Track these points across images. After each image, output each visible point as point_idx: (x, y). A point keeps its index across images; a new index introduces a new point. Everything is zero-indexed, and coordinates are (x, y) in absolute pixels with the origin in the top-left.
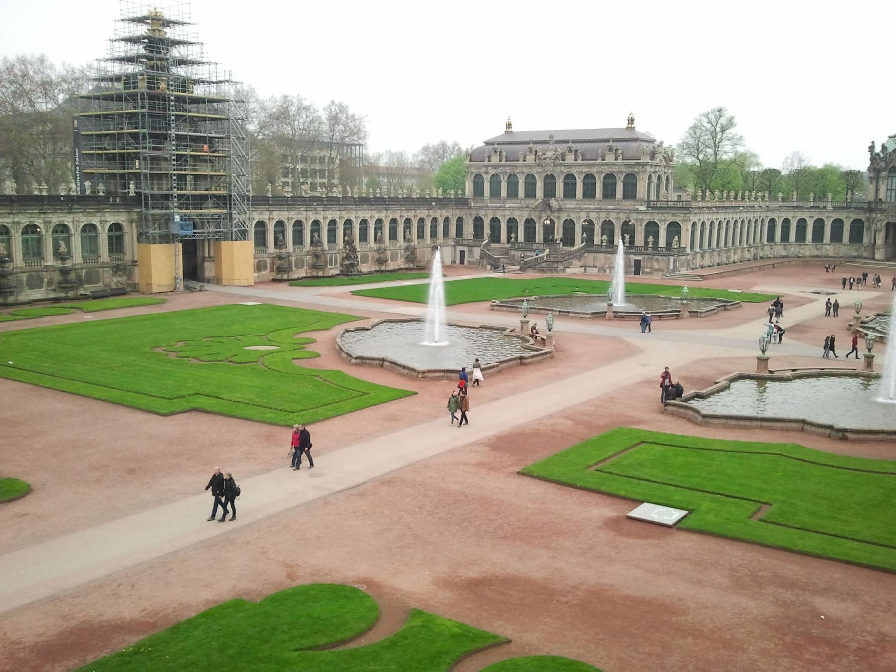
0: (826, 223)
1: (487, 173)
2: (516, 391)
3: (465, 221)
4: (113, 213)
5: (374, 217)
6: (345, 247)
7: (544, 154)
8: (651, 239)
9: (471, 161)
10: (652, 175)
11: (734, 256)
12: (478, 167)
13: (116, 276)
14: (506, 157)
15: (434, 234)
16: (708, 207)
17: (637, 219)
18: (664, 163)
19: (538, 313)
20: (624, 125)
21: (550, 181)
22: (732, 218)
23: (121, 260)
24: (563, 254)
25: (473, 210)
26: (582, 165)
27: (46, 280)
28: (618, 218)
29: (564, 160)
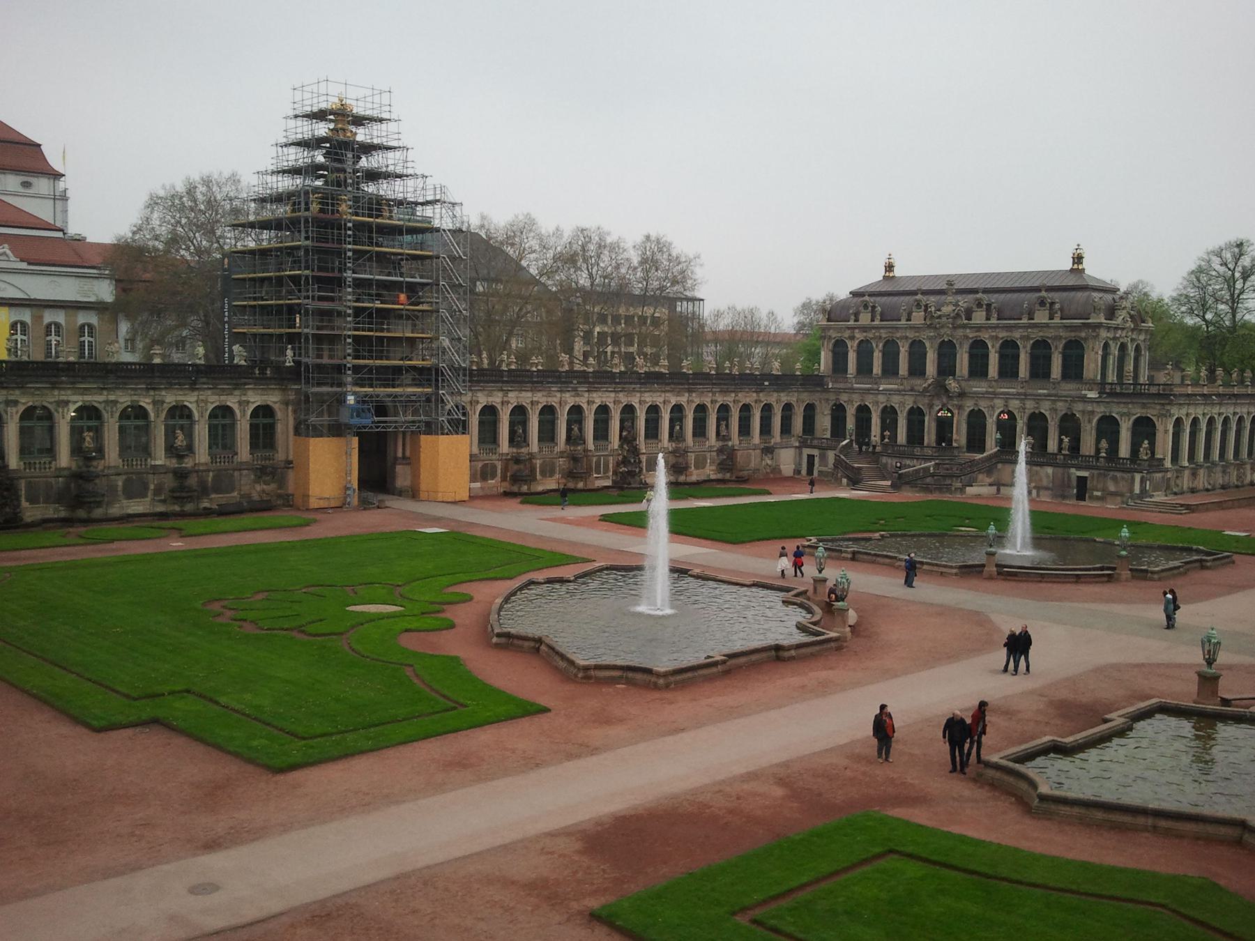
1: (852, 338)
2: (733, 712)
3: (818, 410)
4: (260, 391)
5: (670, 402)
6: (621, 446)
7: (939, 310)
9: (829, 320)
10: (1111, 342)
12: (840, 330)
13: (259, 482)
14: (882, 314)
15: (766, 429)
16: (1204, 395)
17: (1083, 412)
18: (1130, 324)
19: (873, 562)
20: (1068, 265)
21: (947, 352)
23: (270, 460)
24: (961, 465)
25: (831, 394)
27: (152, 487)
29: (970, 319)
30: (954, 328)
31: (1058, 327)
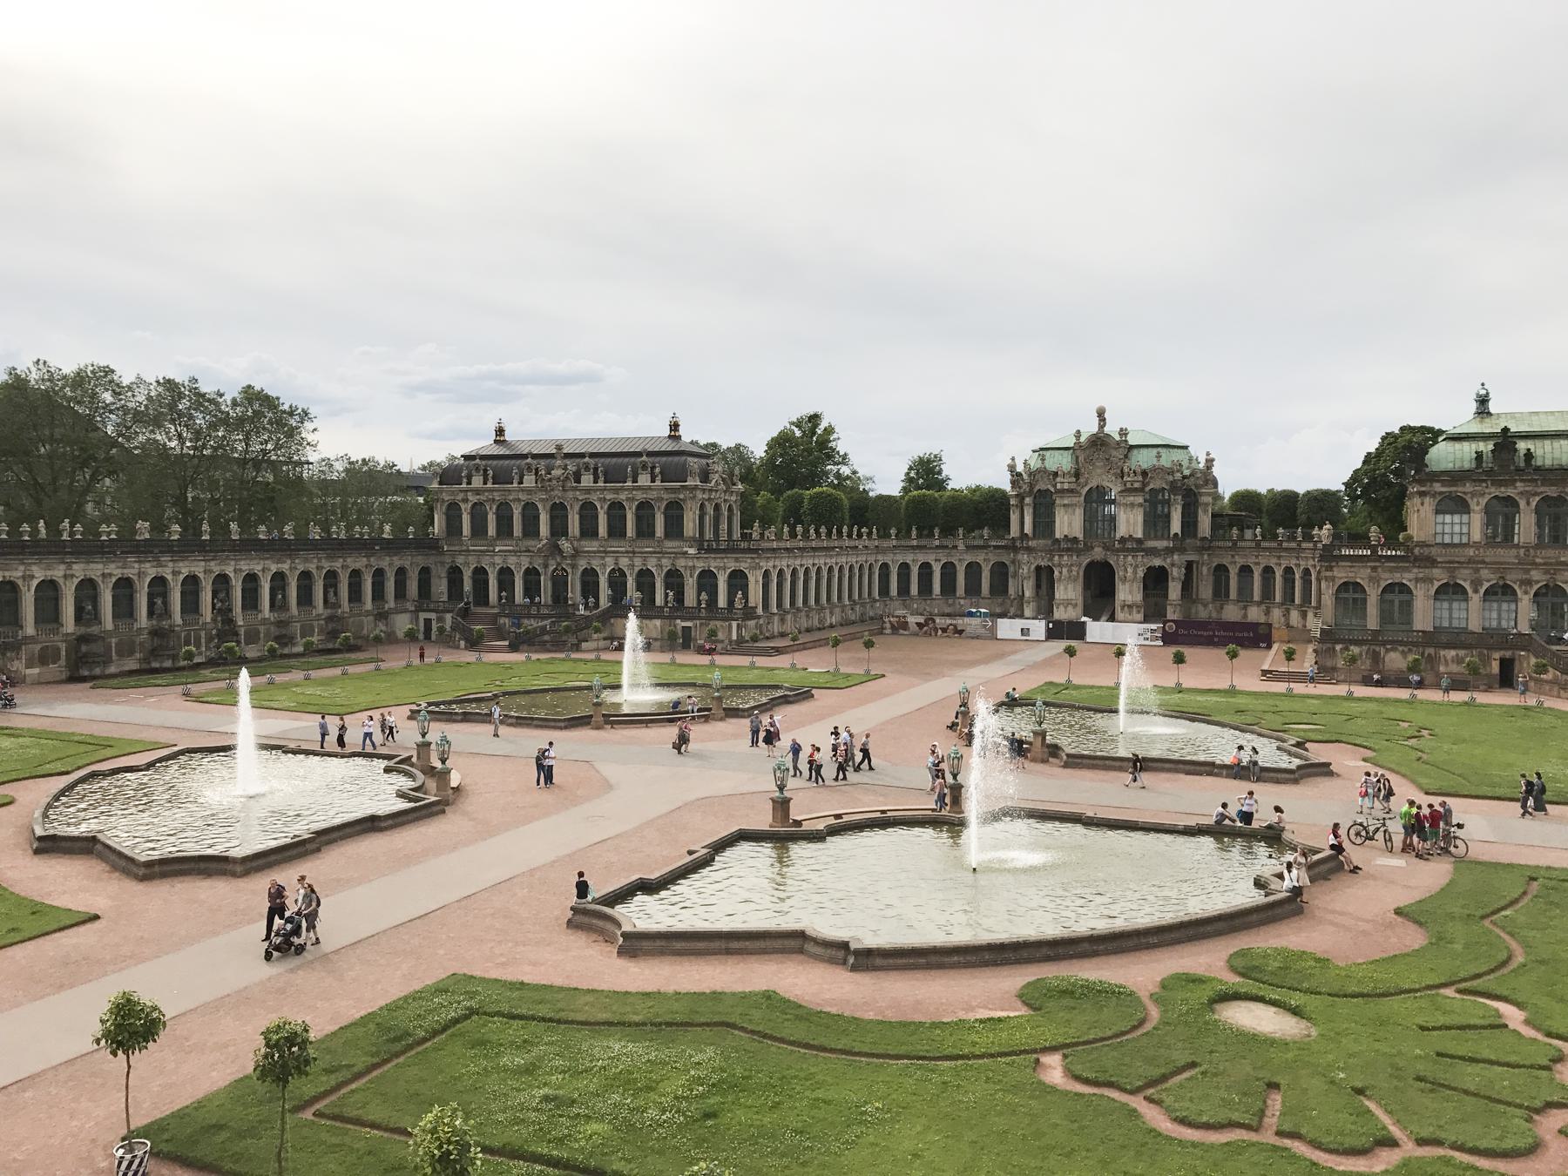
0: (958, 568)
1: (466, 500)
3: (434, 572)
5: (269, 570)
6: (214, 620)
8: (704, 596)
9: (440, 483)
10: (706, 503)
11: (831, 618)
14: (493, 478)
15: (378, 594)
17: (686, 567)
18: (722, 487)
21: (558, 513)
22: (825, 564)
26: (605, 489)
28: (660, 566)
29: (580, 483)
30: (564, 490)
31: (658, 489)
